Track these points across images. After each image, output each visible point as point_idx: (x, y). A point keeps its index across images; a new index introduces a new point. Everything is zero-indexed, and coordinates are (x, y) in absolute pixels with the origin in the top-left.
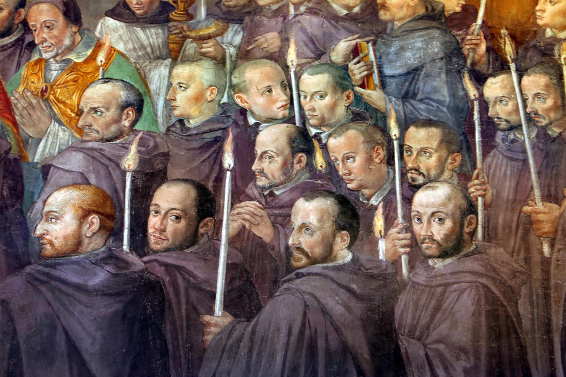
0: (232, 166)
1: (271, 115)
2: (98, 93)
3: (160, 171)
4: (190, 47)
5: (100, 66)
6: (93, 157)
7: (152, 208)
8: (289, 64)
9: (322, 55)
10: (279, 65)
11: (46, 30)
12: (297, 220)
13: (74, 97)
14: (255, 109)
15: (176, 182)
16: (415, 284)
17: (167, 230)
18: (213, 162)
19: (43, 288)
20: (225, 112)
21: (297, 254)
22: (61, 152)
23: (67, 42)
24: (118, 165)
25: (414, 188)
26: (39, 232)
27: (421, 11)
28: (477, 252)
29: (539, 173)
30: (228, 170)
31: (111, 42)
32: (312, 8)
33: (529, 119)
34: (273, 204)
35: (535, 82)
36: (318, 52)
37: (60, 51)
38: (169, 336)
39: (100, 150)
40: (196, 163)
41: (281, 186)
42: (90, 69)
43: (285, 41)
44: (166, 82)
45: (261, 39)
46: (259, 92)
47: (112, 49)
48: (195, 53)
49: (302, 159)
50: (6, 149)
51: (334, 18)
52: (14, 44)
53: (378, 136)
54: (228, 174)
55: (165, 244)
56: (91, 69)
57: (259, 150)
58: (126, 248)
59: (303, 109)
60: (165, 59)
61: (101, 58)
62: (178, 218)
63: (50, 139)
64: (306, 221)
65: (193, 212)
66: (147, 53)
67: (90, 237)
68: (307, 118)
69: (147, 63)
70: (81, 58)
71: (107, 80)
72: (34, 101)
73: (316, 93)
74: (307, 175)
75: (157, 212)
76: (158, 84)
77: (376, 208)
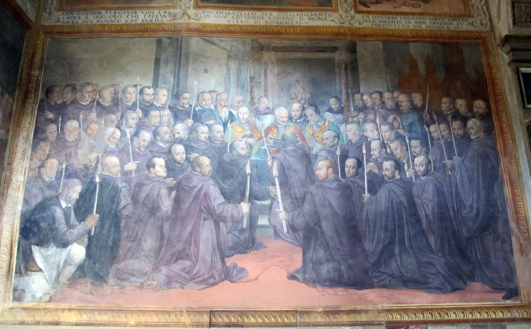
12: (384, 167)
14: (370, 136)
16: (417, 184)
19: (320, 189)
23: (317, 120)
25: (415, 157)
27: (411, 107)
28: (432, 174)
29: (446, 152)
33: (442, 137)
35: (443, 126)
38: (354, 200)
43: (375, 117)
45: (369, 116)
47: (329, 121)
51: (388, 109)
53: (403, 143)
55: (350, 175)
57: (372, 148)
58: (340, 177)
61: (327, 124)
62: (353, 168)
65: (356, 166)
71: (329, 130)
77: (404, 163)
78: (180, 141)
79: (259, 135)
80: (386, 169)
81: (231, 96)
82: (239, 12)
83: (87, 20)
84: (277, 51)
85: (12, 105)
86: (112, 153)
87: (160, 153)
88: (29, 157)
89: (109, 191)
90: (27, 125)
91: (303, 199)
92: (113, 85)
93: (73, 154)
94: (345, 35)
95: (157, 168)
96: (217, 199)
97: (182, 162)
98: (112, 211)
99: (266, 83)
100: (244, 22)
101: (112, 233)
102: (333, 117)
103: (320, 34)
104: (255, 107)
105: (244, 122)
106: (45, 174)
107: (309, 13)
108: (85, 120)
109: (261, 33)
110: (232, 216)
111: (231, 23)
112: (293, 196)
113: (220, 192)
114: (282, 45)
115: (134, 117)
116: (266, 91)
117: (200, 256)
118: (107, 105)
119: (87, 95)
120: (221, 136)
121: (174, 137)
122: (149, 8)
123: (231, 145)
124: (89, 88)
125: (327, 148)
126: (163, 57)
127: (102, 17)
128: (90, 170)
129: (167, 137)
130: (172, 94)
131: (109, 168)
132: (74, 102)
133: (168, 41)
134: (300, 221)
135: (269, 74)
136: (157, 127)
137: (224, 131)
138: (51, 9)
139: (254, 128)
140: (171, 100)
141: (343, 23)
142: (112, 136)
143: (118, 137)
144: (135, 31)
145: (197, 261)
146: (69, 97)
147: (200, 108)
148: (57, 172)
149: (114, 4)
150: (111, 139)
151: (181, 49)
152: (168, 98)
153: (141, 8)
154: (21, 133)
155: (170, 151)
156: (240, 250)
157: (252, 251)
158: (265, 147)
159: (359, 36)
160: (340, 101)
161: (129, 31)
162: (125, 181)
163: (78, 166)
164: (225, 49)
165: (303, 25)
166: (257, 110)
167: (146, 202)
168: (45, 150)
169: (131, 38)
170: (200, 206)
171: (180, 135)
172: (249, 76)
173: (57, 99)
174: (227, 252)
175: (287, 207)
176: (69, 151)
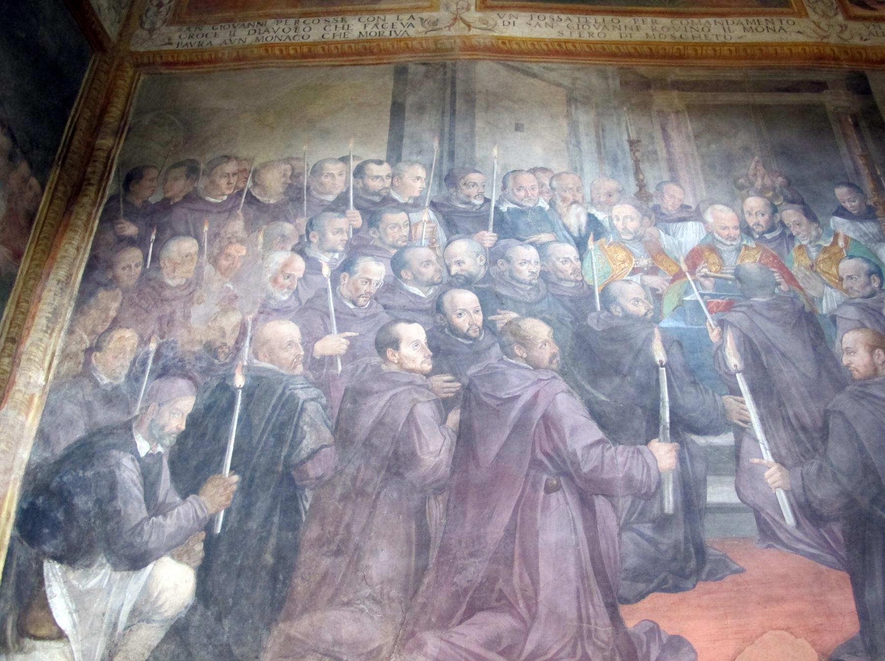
19: (863, 402)
22: (839, 306)
23: (814, 233)
42: (836, 251)
61: (841, 243)
72: (808, 273)
78: (467, 282)
79: (674, 269)
81: (588, 178)
82: (583, 18)
83: (233, 38)
84: (683, 90)
85: (37, 198)
86: (281, 312)
87: (412, 312)
88: (66, 326)
89: (269, 410)
90: (72, 251)
91: (824, 432)
92: (288, 160)
93: (179, 315)
94: (836, 59)
95: (406, 349)
96: (581, 434)
97: (472, 334)
98: (276, 464)
99: (669, 152)
100: (595, 35)
101: (275, 530)
102: (852, 228)
103: (776, 56)
104: (651, 205)
105: (630, 237)
106: (100, 368)
107: (743, 20)
108: (215, 236)
109: (640, 56)
110: (629, 480)
111: (567, 36)
112: (793, 421)
113: (587, 414)
114: (694, 79)
115: (339, 229)
117: (541, 597)
118: (272, 201)
119: (223, 182)
120: (574, 271)
121: (449, 271)
122: (375, 11)
123: (604, 292)
124: (231, 167)
125: (857, 300)
126: (411, 100)
127: (267, 31)
128: (222, 357)
129: (429, 272)
130: (438, 175)
131: (271, 352)
132: (191, 198)
133: (423, 69)
134: (825, 493)
135: (673, 134)
136: (402, 250)
137: (581, 259)
138: (153, 23)
139: (658, 254)
140: (436, 188)
141: (825, 37)
142: (282, 272)
143: (300, 274)
144: (343, 54)
145: (534, 617)
146: (179, 186)
147: (512, 206)
148: (133, 363)
149: (296, 7)
150: (281, 280)
151: (453, 84)
152: (428, 184)
153: (355, 12)
154: (54, 270)
155: (438, 307)
156: (664, 581)
157: (701, 586)
158: (695, 296)
159: (868, 61)
160: (862, 192)
161: (330, 55)
162: (317, 385)
163: (188, 347)
164: (559, 85)
165: (733, 41)
166: (656, 209)
167: (375, 441)
168: (107, 309)
169: (334, 66)
170: (533, 450)
171: (464, 266)
172: (625, 137)
173: (150, 193)
174: (625, 588)
175: (783, 452)
176: (168, 310)
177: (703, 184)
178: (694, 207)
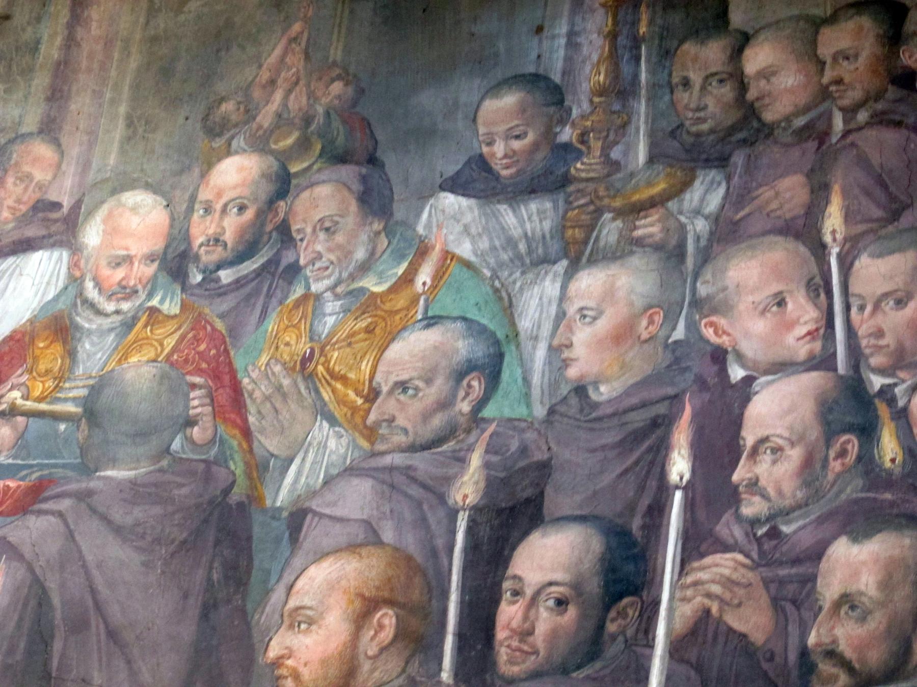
0: (687, 477)
1: (780, 354)
2: (413, 348)
3: (528, 501)
4: (610, 230)
5: (421, 294)
6: (392, 486)
7: (507, 585)
8: (828, 238)
9: (904, 209)
10: (804, 243)
11: (322, 236)
12: (829, 589)
13: (364, 363)
14: (749, 348)
15: (562, 523)
17: (537, 631)
18: (644, 472)
20: (677, 360)
21: (826, 667)
22: (326, 483)
23: (360, 254)
24: (442, 499)
26: (272, 653)
30: (677, 487)
31: (446, 243)
32: (883, 113)
34: (777, 555)
36: (894, 206)
37: (345, 275)
39: (408, 472)
40: (608, 478)
41: (796, 513)
43: (819, 193)
44: (553, 309)
46: (756, 308)
47: (448, 256)
48: (619, 242)
49: (849, 447)
50: (222, 485)
52: (259, 273)
54: (678, 496)
55: (531, 663)
56: (402, 301)
57: (749, 437)
59: (856, 334)
60: (555, 263)
61: (424, 277)
62: (561, 603)
63: (311, 456)
64: (853, 588)
65: (594, 586)
66: (519, 257)
67: (375, 658)
68: (862, 354)
69: (518, 274)
70: (385, 282)
71: (431, 321)
72: (286, 382)
73: (886, 295)
74: (859, 482)
75: (516, 593)
76: (537, 315)
80: (847, 601)
99: (71, 42)
116: (57, 95)
177: (119, 131)
178: (66, 203)
